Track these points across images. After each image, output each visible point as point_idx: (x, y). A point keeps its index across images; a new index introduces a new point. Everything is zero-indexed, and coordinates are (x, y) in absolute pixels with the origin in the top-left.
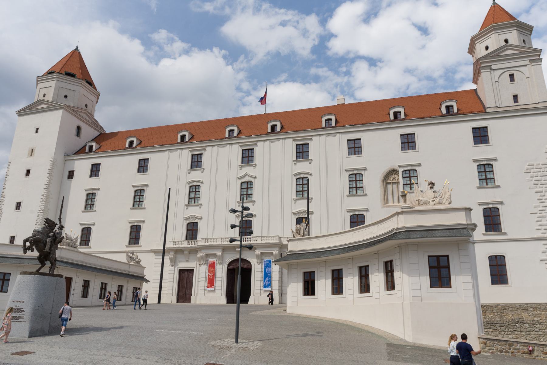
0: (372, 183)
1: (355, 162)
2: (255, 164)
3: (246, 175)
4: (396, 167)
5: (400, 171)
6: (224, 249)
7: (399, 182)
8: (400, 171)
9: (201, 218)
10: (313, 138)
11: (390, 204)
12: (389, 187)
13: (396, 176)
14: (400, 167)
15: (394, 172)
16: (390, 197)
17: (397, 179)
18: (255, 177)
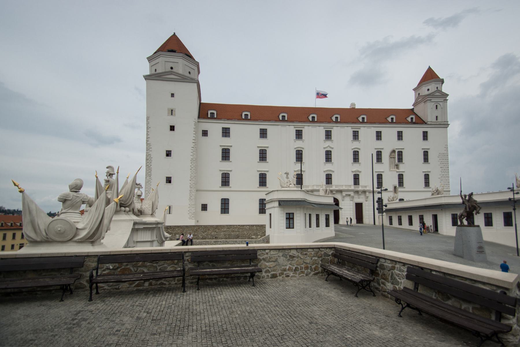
0: (385, 156)
1: (379, 145)
5: (397, 151)
8: (397, 151)
15: (394, 151)
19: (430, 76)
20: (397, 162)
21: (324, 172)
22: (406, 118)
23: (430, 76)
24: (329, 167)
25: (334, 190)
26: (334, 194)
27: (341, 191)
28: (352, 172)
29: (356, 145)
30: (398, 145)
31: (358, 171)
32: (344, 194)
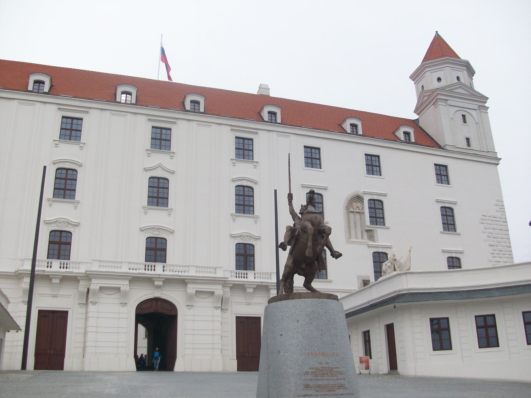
2: (174, 153)
3: (159, 166)
4: (361, 194)
5: (366, 198)
6: (135, 280)
7: (363, 213)
8: (366, 198)
9: (77, 225)
10: (260, 132)
11: (353, 239)
12: (351, 215)
13: (359, 204)
14: (365, 193)
15: (358, 198)
16: (353, 231)
17: (361, 208)
18: (173, 173)
19: (439, 51)
20: (368, 222)
21: (142, 230)
22: (394, 133)
23: (439, 51)
24: (157, 218)
25: (159, 277)
26: (158, 287)
27: (183, 282)
28: (232, 236)
29: (244, 171)
30: (371, 186)
31: (251, 237)
32: (192, 288)
